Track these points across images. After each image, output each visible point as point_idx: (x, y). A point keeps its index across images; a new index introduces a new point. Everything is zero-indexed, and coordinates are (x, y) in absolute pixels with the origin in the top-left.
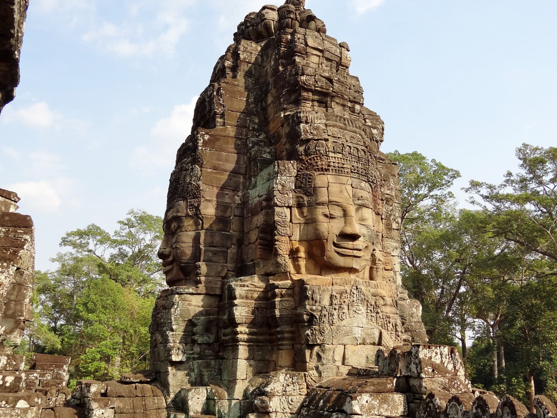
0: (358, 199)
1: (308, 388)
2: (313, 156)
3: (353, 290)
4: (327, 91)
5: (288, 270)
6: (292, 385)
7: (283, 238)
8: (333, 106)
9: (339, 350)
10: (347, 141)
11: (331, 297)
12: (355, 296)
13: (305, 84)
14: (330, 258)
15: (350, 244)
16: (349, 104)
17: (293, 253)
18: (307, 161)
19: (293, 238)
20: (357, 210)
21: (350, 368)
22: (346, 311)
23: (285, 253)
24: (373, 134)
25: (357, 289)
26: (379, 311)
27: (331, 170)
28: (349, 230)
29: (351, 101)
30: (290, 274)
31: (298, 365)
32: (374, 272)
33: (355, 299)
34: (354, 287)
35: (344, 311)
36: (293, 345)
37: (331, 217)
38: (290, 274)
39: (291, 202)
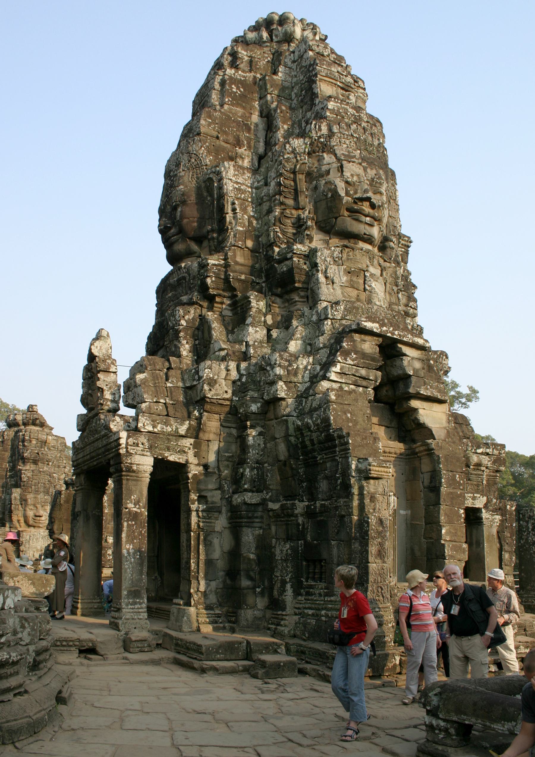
9: (31, 553)
15: (38, 518)
28: (37, 514)
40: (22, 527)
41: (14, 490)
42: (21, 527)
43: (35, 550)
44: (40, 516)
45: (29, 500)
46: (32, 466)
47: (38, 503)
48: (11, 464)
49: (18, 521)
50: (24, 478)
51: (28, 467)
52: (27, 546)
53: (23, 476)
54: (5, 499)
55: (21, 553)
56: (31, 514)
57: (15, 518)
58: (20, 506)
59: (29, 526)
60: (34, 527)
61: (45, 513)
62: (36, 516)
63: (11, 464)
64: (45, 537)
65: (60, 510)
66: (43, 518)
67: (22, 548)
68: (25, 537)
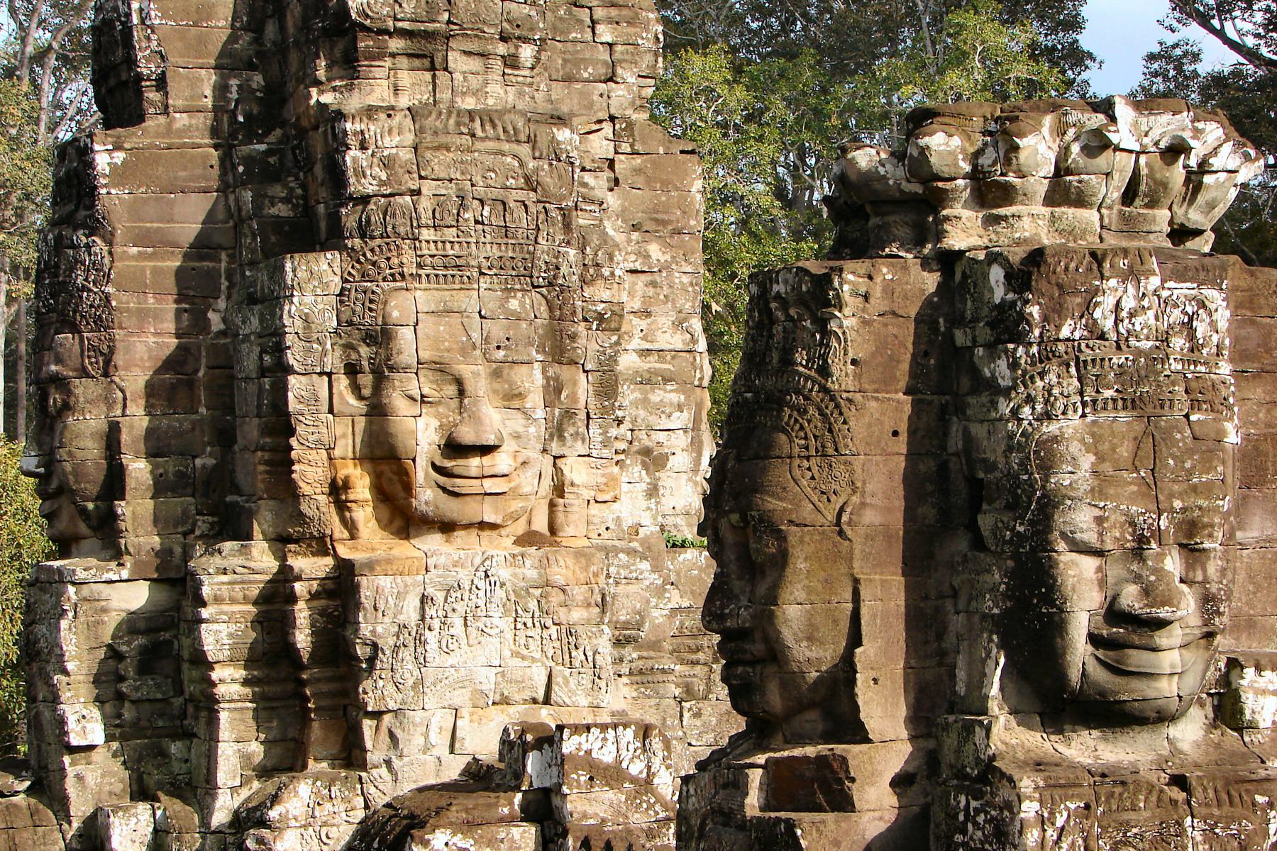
0: (498, 347)
1: (367, 807)
2: (378, 241)
4: (431, 27)
6: (328, 805)
7: (313, 455)
8: (451, 65)
10: (473, 185)
11: (424, 599)
12: (481, 593)
13: (367, 16)
15: (474, 464)
16: (502, 49)
18: (364, 255)
20: (496, 374)
21: (469, 758)
22: (458, 629)
24: (558, 143)
25: (487, 576)
26: (549, 623)
27: (424, 278)
28: (467, 435)
29: (504, 38)
31: (351, 756)
32: (560, 517)
33: (481, 603)
35: (452, 631)
36: (345, 707)
40: (369, 539)
41: (296, 268)
43: (461, 698)
44: (486, 450)
45: (405, 335)
46: (405, 78)
47: (467, 349)
48: (258, 80)
49: (338, 491)
50: (364, 171)
51: (376, 90)
52: (408, 670)
53: (353, 156)
54: (229, 331)
55: (368, 725)
56: (421, 433)
57: (310, 474)
58: (342, 383)
59: (404, 519)
60: (447, 527)
61: (516, 422)
63: (258, 80)
64: (520, 595)
65: (828, 448)
66: (501, 461)
67: (375, 692)
68: (387, 605)
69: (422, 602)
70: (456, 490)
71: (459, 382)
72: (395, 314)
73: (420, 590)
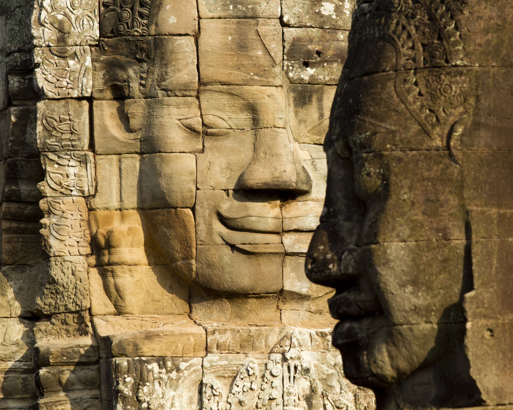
3: (270, 366)
5: (86, 304)
14: (210, 265)
17: (101, 250)
19: (97, 202)
23: (74, 250)
30: (91, 315)
34: (273, 356)
37: (205, 133)
38: (91, 315)
39: (89, 84)
42: (115, 295)
62: (246, 192)
69: (200, 392)
70: (246, 248)
71: (252, 109)
72: (172, 20)
73: (195, 377)
